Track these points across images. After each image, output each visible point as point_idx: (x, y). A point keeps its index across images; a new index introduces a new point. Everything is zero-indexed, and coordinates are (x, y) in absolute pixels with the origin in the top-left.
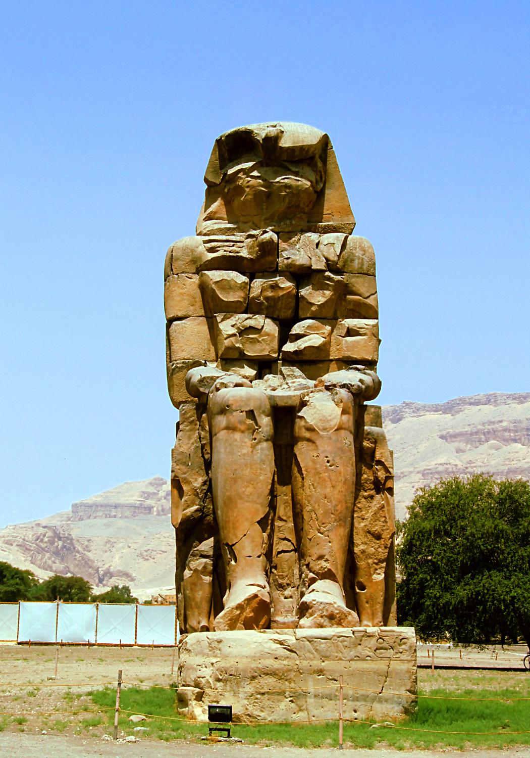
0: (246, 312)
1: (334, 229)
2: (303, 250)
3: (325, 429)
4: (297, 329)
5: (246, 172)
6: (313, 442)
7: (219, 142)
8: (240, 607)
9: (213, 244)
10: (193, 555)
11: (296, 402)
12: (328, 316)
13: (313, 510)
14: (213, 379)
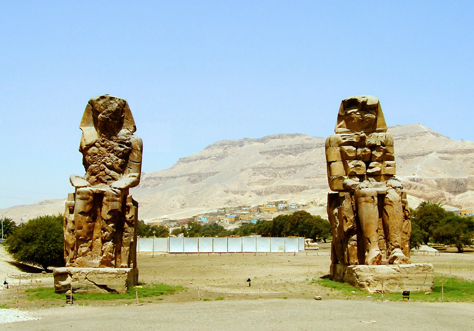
1: (381, 131)
2: (373, 139)
3: (395, 202)
4: (371, 165)
6: (392, 206)
8: (376, 258)
10: (351, 240)
11: (385, 193)
12: (381, 160)
13: (393, 227)
14: (356, 185)
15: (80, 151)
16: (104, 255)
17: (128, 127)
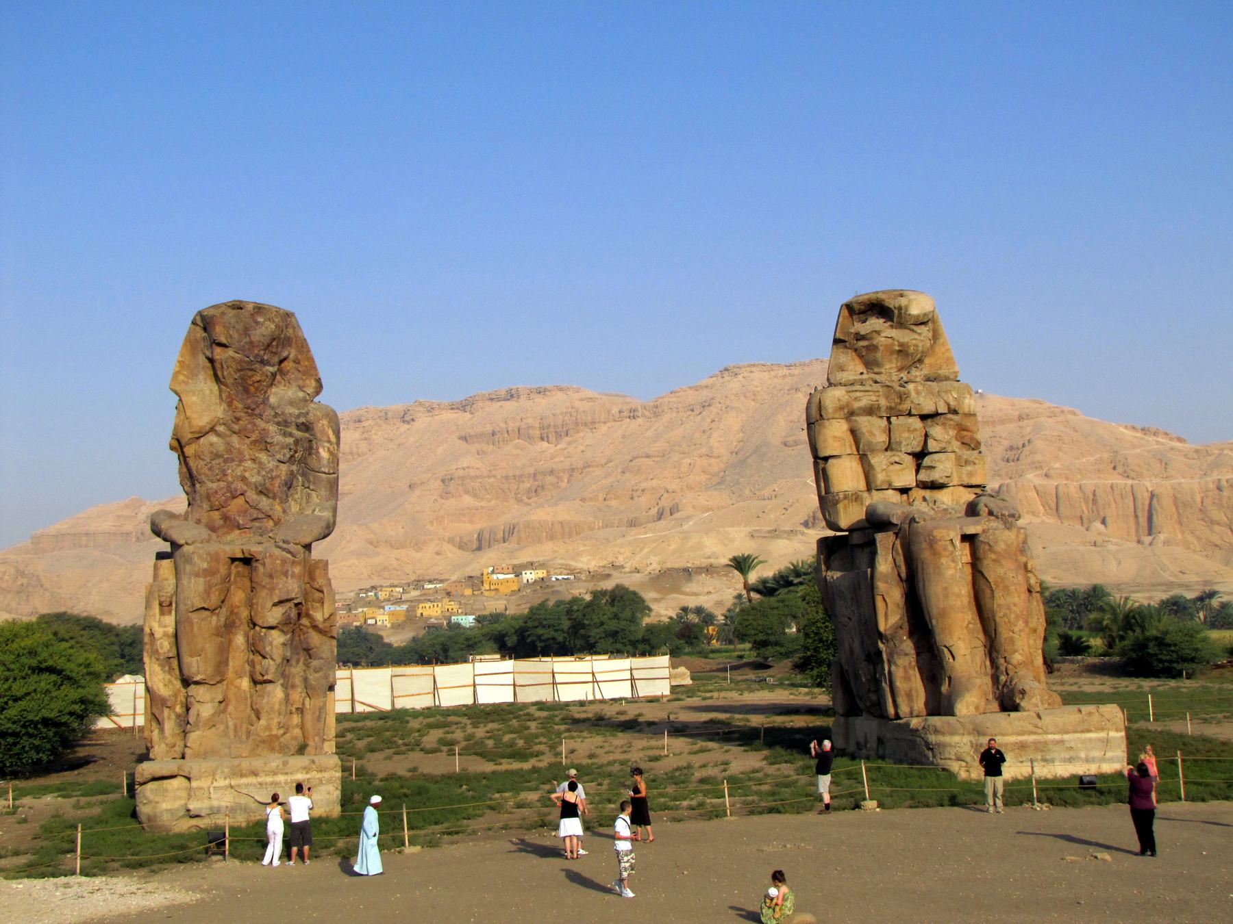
0: (886, 450)
4: (927, 461)
5: (878, 333)
7: (849, 307)
9: (858, 394)
15: (172, 448)
16: (263, 722)
17: (301, 382)
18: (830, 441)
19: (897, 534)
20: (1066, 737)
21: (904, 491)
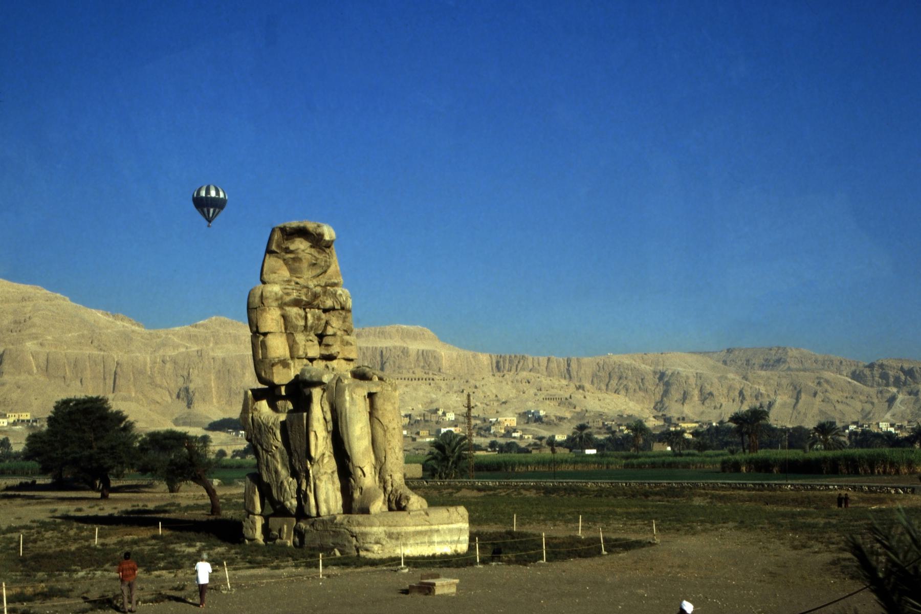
4: (326, 340)
18: (269, 321)
19: (324, 390)
20: (441, 527)
21: (311, 360)
